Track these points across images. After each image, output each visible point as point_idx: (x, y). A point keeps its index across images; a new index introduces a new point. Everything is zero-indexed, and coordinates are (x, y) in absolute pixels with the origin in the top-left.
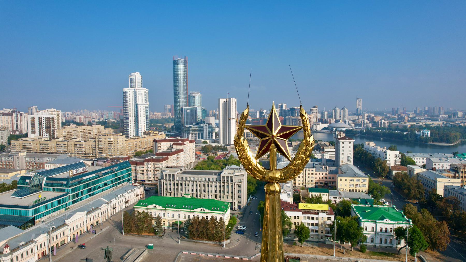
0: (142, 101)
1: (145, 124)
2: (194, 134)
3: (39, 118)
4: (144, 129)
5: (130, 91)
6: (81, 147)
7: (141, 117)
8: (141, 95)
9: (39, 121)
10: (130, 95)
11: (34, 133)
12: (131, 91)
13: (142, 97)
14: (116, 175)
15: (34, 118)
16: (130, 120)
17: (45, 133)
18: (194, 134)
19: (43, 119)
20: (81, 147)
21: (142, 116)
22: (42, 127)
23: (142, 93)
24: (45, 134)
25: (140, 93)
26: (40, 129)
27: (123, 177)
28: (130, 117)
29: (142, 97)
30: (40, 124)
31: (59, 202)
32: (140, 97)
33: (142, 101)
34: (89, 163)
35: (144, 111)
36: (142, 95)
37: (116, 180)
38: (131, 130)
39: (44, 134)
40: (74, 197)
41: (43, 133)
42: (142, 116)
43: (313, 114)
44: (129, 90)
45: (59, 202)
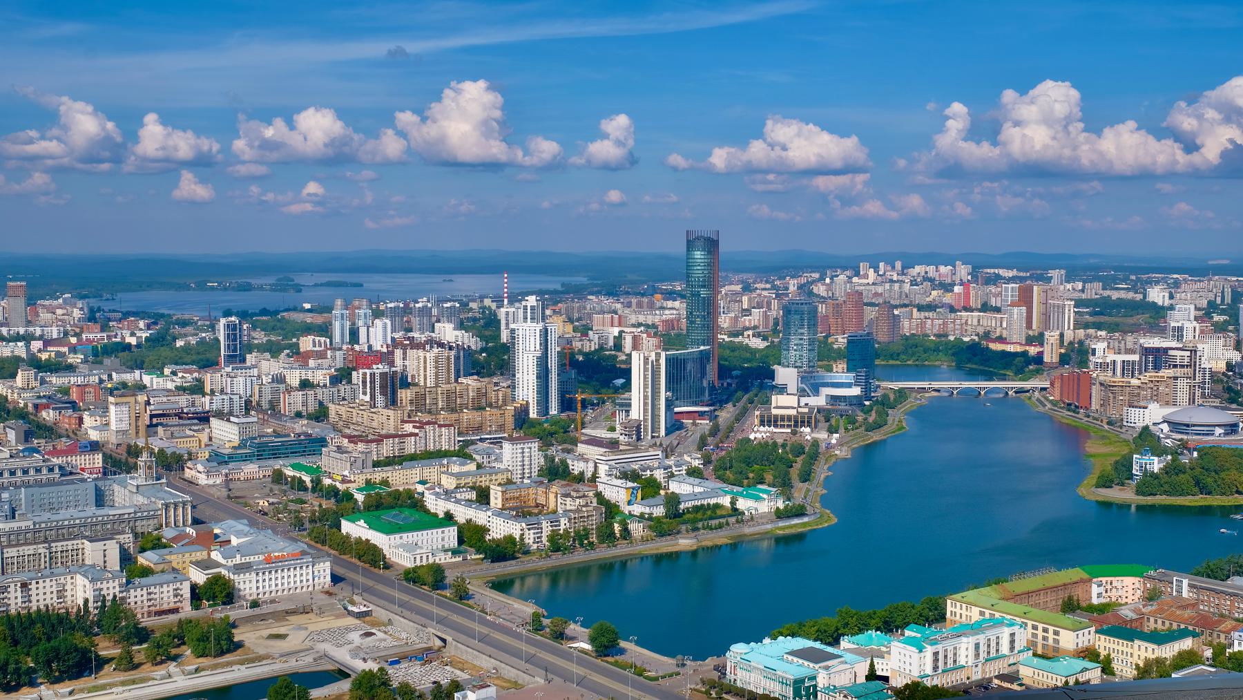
1: (535, 388)
9: (371, 378)
11: (364, 393)
12: (521, 328)
14: (306, 447)
15: (365, 374)
26: (373, 388)
27: (314, 451)
30: (373, 382)
31: (246, 456)
32: (532, 338)
34: (293, 435)
37: (304, 451)
40: (258, 456)
43: (1166, 373)
45: (246, 456)
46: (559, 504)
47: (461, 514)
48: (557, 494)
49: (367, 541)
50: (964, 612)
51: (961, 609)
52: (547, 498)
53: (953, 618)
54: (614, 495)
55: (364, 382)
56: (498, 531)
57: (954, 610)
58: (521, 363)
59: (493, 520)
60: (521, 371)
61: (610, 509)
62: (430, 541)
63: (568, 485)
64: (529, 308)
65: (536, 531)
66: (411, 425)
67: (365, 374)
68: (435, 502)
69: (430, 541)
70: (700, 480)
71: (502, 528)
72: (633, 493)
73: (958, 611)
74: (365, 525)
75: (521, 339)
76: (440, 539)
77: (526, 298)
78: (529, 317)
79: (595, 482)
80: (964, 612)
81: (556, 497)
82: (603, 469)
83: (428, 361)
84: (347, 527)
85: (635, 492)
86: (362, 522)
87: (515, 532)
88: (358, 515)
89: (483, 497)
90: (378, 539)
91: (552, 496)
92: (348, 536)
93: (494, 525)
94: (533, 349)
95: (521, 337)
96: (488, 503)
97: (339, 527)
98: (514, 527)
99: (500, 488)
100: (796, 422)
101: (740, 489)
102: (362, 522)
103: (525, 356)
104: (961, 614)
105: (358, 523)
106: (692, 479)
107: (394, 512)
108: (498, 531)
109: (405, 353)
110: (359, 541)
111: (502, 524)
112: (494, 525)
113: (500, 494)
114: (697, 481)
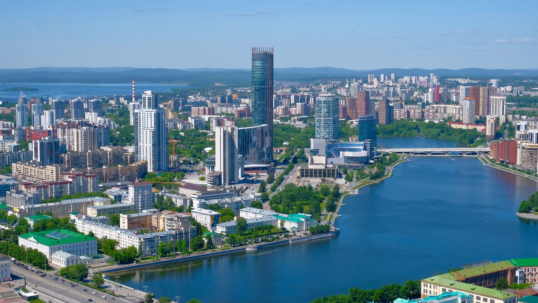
0: (151, 125)
1: (151, 152)
2: (211, 167)
3: (40, 143)
4: (150, 157)
5: (140, 113)
6: (41, 173)
7: (146, 143)
8: (149, 117)
9: (40, 146)
10: (140, 117)
12: (141, 112)
13: (151, 119)
15: (36, 144)
16: (140, 146)
17: (46, 158)
18: (211, 167)
19: (44, 144)
20: (41, 173)
21: (148, 142)
22: (43, 152)
23: (151, 115)
24: (46, 158)
25: (149, 115)
28: (140, 142)
29: (151, 119)
32: (149, 119)
33: (151, 125)
35: (150, 137)
36: (151, 117)
38: (140, 158)
39: (45, 158)
41: (44, 157)
42: (148, 142)
44: (140, 112)
46: (166, 226)
47: (100, 233)
48: (164, 219)
49: (36, 250)
50: (432, 290)
51: (431, 287)
52: (158, 222)
53: (425, 294)
54: (203, 220)
55: (36, 149)
56: (125, 243)
57: (426, 288)
58: (142, 135)
59: (122, 236)
60: (142, 141)
61: (199, 229)
62: (78, 250)
63: (172, 213)
64: (147, 99)
65: (150, 243)
66: (67, 176)
67: (36, 144)
68: (83, 226)
69: (78, 250)
70: (261, 210)
71: (128, 241)
72: (215, 218)
73: (428, 289)
74: (34, 240)
75: (141, 120)
76: (85, 249)
77: (145, 92)
78: (147, 105)
79: (190, 212)
80: (432, 290)
81: (164, 221)
82: (196, 203)
83: (80, 135)
84: (22, 241)
85: (217, 218)
86: (32, 239)
87: (135, 243)
88: (29, 234)
89: (116, 222)
90: (44, 249)
91: (161, 221)
92: (23, 247)
93: (122, 239)
94: (149, 126)
95: (141, 118)
96: (119, 226)
97: (17, 242)
98: (135, 240)
99: (126, 216)
100: (325, 174)
101: (286, 216)
102: (32, 239)
103: (145, 131)
104: (430, 292)
105: (30, 239)
106: (255, 209)
107: (54, 232)
108: (125, 243)
109: (64, 132)
110: (30, 250)
111: (128, 238)
112: (122, 239)
113: (126, 220)
114: (259, 210)
